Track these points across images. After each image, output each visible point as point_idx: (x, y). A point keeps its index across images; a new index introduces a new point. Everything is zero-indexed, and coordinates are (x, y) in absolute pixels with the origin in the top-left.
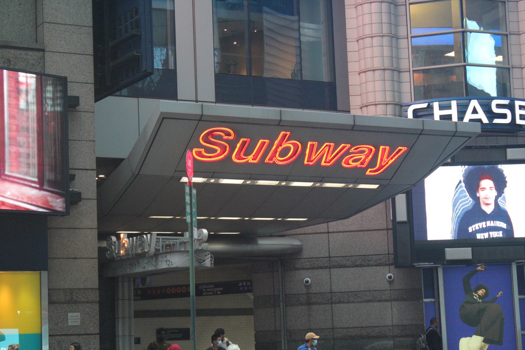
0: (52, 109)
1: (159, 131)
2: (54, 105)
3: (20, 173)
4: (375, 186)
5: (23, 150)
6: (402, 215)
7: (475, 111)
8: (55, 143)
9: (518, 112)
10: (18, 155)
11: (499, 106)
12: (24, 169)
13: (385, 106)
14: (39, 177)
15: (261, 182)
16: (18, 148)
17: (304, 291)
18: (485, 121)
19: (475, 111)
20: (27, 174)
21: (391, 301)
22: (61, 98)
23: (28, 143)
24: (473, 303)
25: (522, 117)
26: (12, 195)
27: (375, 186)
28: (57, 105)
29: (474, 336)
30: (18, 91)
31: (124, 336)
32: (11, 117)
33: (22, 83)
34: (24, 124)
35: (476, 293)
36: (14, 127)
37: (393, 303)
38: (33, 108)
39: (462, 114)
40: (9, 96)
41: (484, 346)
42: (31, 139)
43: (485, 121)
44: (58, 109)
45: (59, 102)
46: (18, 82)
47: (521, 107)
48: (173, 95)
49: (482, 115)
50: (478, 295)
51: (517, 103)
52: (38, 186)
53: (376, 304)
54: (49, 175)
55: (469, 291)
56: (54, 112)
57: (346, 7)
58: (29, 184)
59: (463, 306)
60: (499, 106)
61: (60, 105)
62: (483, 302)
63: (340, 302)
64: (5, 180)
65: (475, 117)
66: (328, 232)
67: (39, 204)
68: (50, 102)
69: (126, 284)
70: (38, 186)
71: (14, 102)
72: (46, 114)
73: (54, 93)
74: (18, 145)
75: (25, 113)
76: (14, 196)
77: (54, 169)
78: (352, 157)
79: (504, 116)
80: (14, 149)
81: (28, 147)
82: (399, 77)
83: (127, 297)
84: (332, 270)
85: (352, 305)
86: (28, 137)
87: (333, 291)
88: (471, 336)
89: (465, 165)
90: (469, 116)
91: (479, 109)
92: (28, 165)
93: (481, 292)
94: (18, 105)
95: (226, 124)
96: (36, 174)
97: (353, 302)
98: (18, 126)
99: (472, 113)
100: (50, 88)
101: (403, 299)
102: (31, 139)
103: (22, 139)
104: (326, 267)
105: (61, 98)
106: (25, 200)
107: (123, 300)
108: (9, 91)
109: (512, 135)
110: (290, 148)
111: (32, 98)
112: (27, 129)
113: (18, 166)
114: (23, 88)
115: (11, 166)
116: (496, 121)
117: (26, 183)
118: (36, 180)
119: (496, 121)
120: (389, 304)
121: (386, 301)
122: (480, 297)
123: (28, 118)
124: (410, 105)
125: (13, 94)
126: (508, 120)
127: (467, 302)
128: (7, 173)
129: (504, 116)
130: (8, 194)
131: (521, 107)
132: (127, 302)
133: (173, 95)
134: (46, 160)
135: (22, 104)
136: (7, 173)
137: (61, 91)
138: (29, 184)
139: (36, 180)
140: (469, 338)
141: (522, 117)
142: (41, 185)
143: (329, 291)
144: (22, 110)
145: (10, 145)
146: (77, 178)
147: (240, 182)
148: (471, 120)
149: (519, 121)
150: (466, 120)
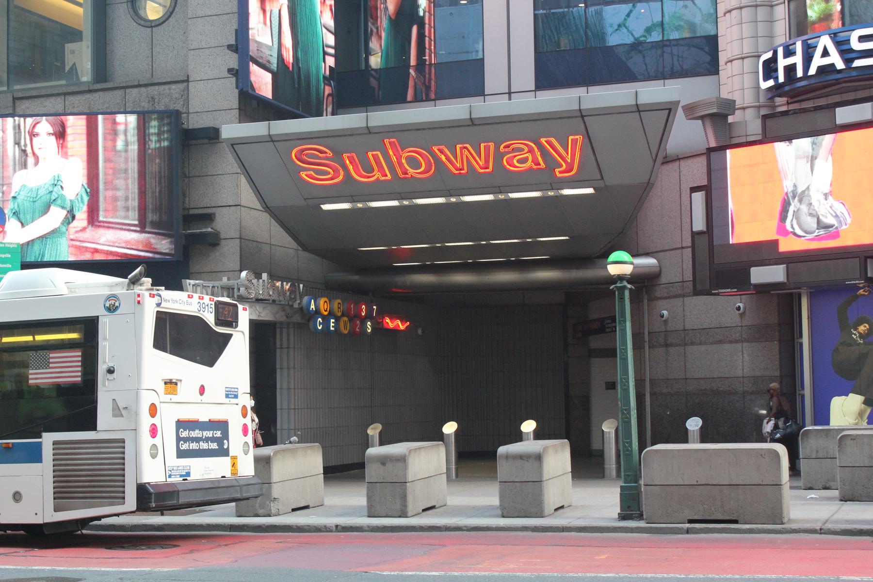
0: (158, 145)
1: (664, 122)
2: (159, 141)
3: (117, 218)
4: (590, 191)
5: (120, 194)
6: (699, 224)
7: (825, 53)
8: (160, 183)
10: (115, 199)
12: (122, 213)
14: (139, 220)
15: (567, 192)
16: (114, 192)
17: (663, 329)
18: (840, 65)
19: (825, 53)
20: (126, 217)
21: (742, 342)
22: (168, 131)
23: (127, 185)
24: (850, 345)
26: (107, 241)
27: (590, 191)
28: (164, 140)
29: (851, 395)
30: (115, 133)
31: (281, 389)
32: (106, 160)
33: (119, 124)
34: (123, 166)
35: (856, 329)
36: (111, 172)
37: (745, 344)
38: (134, 147)
39: (808, 60)
40: (105, 138)
41: (865, 411)
42: (130, 181)
43: (840, 65)
44: (166, 144)
45: (166, 136)
46: (115, 123)
48: (479, 91)
50: (859, 333)
52: (138, 229)
53: (727, 346)
54: (150, 217)
55: (846, 326)
56: (160, 148)
58: (128, 227)
59: (837, 349)
61: (167, 139)
62: (865, 343)
63: (693, 343)
64: (99, 226)
65: (826, 61)
66: (683, 248)
67: (140, 248)
68: (154, 138)
69: (285, 330)
70: (138, 229)
71: (110, 143)
72: (150, 151)
73: (159, 127)
74: (116, 189)
75: (123, 154)
76: (111, 241)
77: (158, 209)
78: (515, 156)
80: (110, 193)
81: (127, 189)
82: (772, 14)
83: (285, 345)
84: (686, 299)
85: (703, 347)
86: (126, 179)
87: (687, 328)
88: (847, 395)
90: (818, 61)
91: (832, 49)
92: (127, 209)
93: (862, 328)
94: (115, 146)
95: (315, 140)
96: (137, 217)
97: (705, 343)
98: (114, 169)
100: (154, 123)
101: (748, 341)
102: (130, 181)
103: (120, 183)
104: (677, 296)
105: (168, 131)
106: (123, 245)
107: (281, 348)
108: (105, 134)
110: (407, 158)
111: (133, 137)
112: (126, 171)
113: (115, 210)
114: (121, 128)
115: (106, 210)
116: (858, 63)
117: (124, 227)
118: (136, 222)
119: (858, 63)
120: (739, 346)
121: (736, 342)
122: (861, 336)
123: (126, 159)
125: (110, 137)
127: (842, 344)
128: (101, 219)
130: (102, 240)
132: (285, 351)
133: (479, 91)
134: (149, 201)
135: (120, 144)
136: (101, 219)
137: (169, 124)
138: (128, 227)
139: (136, 222)
140: (844, 397)
142: (142, 227)
143: (682, 328)
144: (120, 151)
145: (106, 189)
146: (217, 215)
147: (489, 197)
148: (821, 69)
150: (812, 71)
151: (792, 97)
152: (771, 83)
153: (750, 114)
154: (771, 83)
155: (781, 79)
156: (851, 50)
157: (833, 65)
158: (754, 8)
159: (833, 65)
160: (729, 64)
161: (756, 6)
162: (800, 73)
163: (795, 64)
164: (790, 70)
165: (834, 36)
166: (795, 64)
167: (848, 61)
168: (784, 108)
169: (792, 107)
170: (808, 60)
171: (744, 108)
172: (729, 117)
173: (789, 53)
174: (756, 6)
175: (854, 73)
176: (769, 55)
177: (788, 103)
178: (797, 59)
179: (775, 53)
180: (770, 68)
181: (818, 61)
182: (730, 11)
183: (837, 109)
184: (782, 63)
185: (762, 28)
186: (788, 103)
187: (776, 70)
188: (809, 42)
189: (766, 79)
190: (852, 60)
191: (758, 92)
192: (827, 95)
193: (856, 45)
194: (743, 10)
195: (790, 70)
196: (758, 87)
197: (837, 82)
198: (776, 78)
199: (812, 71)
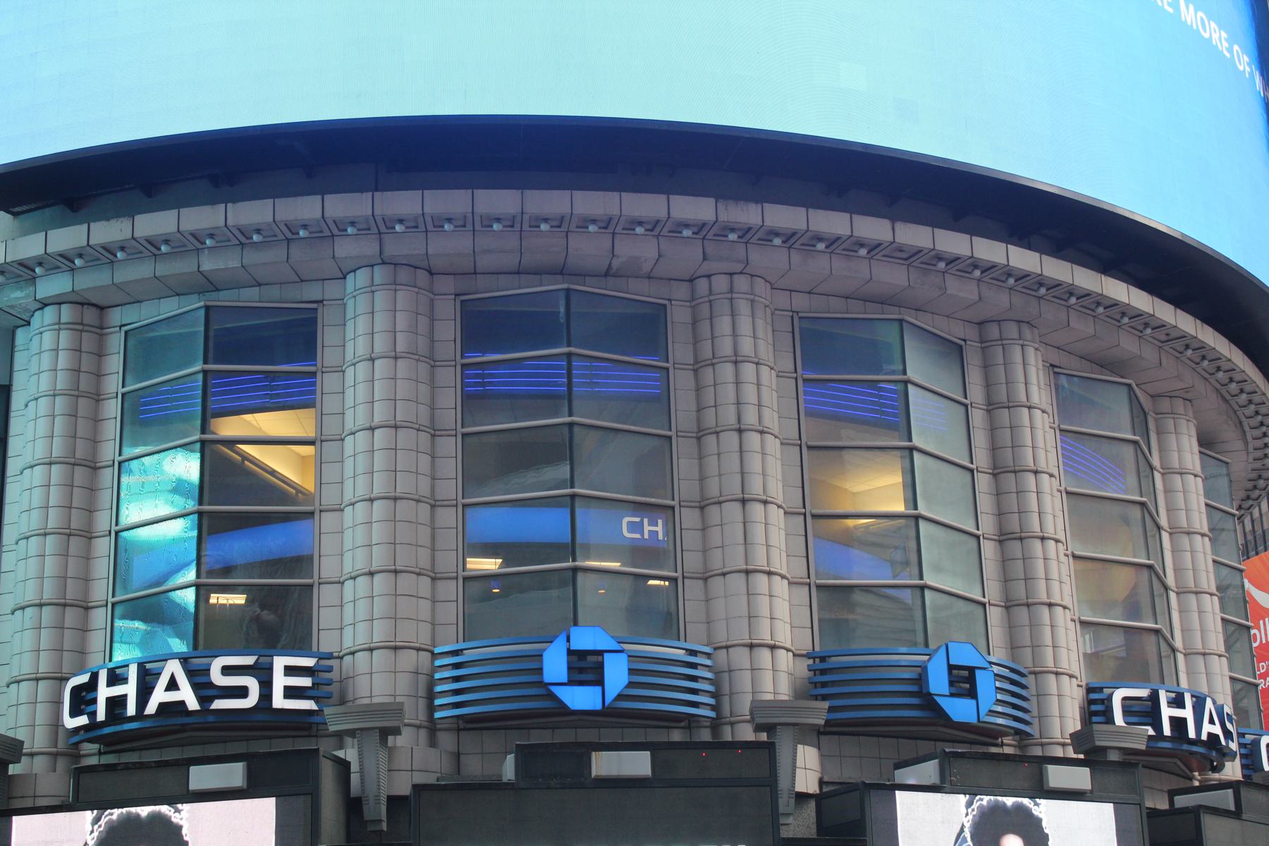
7: (172, 685)
9: (280, 681)
11: (227, 670)
13: (34, 683)
18: (193, 704)
19: (172, 685)
25: (290, 692)
39: (145, 692)
43: (193, 704)
47: (290, 671)
49: (187, 695)
51: (280, 663)
57: (8, 480)
60: (227, 670)
79: (242, 692)
82: (86, 619)
89: (92, 810)
90: (160, 695)
99: (178, 689)
109: (305, 733)
116: (219, 704)
119: (219, 704)
124: (68, 679)
126: (251, 701)
129: (242, 692)
131: (290, 671)
141: (290, 692)
148: (163, 707)
149: (279, 701)
150: (151, 708)
151: (107, 745)
152: (83, 720)
153: (40, 764)
154: (83, 720)
155: (101, 716)
156: (211, 685)
157: (183, 703)
158: (60, 608)
159: (183, 703)
160: (14, 686)
161: (65, 605)
162: (131, 710)
163: (126, 696)
164: (116, 704)
165: (184, 660)
166: (126, 696)
167: (204, 700)
168: (93, 761)
169: (109, 759)
170: (145, 692)
171: (32, 755)
172: (11, 766)
173: (116, 678)
174: (65, 605)
175: (211, 718)
176: (84, 679)
177: (100, 753)
178: (130, 690)
179: (94, 677)
180: (83, 699)
181: (160, 695)
182: (23, 608)
183: (192, 768)
184: (104, 692)
185: (69, 639)
186: (100, 753)
187: (94, 701)
188: (148, 666)
189: (74, 713)
190: (211, 699)
191: (57, 733)
192: (159, 747)
193: (218, 679)
194: (44, 608)
195: (116, 704)
196: (57, 723)
197: (183, 728)
198: (93, 715)
199: (151, 708)
